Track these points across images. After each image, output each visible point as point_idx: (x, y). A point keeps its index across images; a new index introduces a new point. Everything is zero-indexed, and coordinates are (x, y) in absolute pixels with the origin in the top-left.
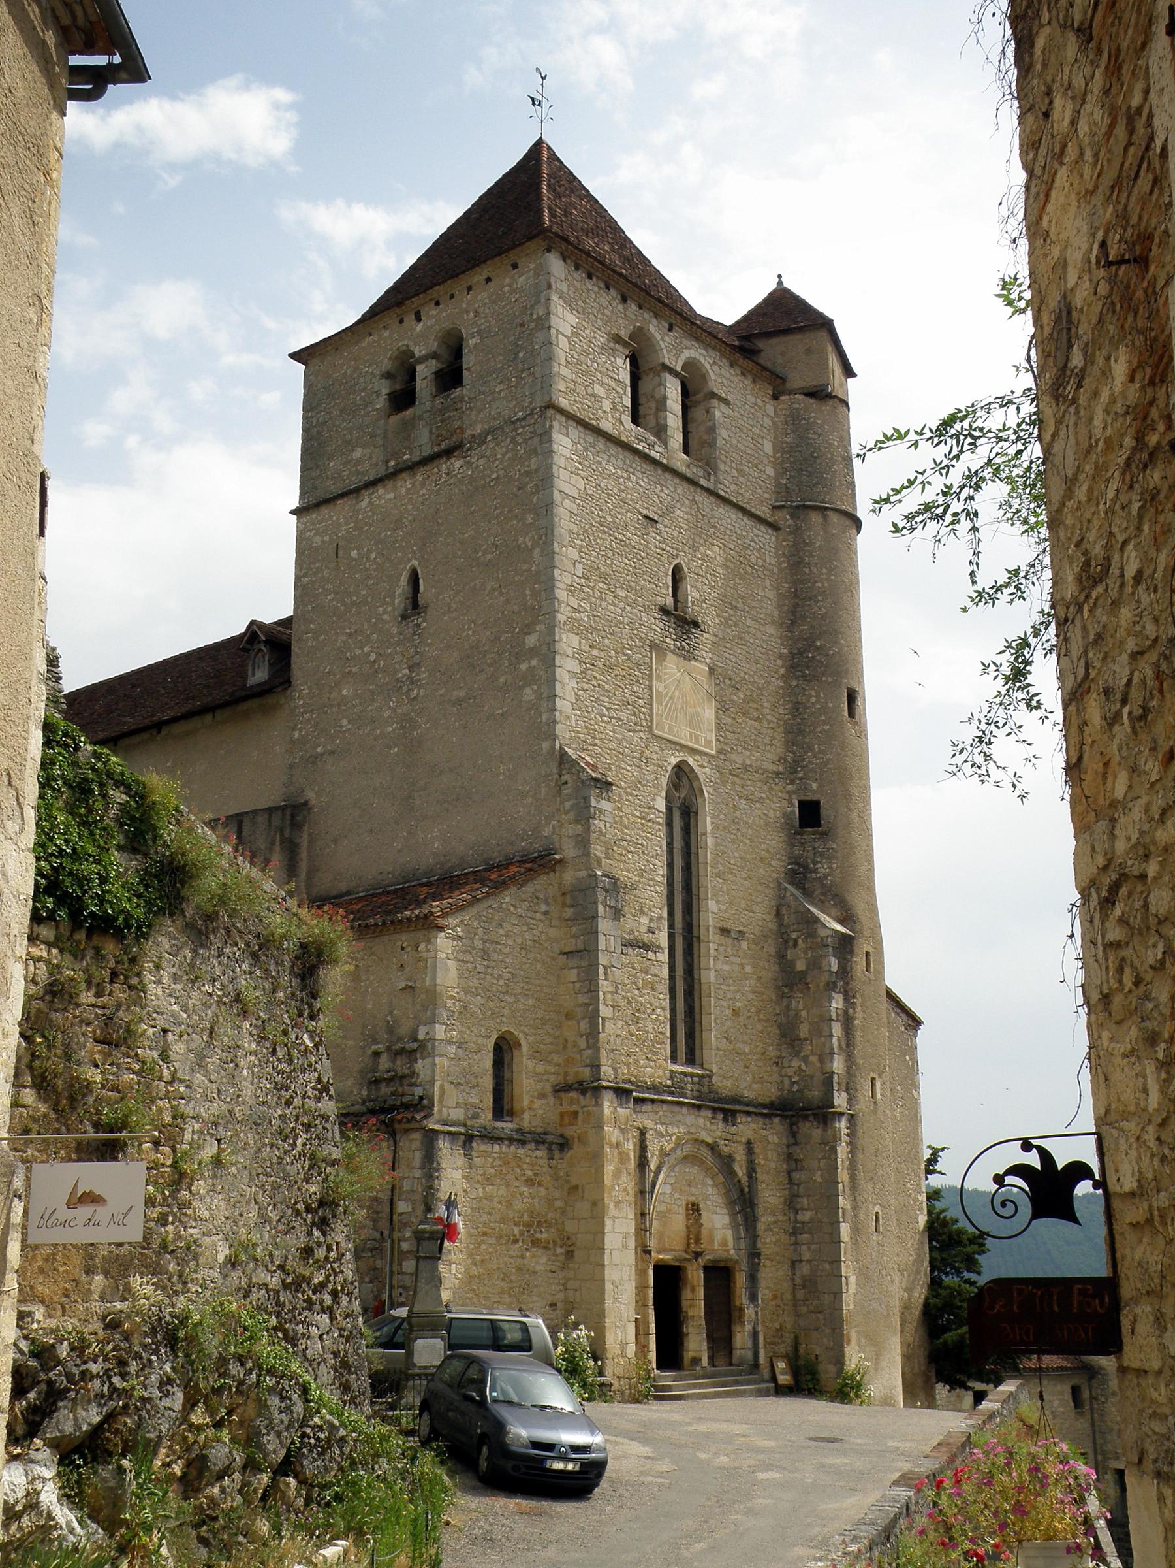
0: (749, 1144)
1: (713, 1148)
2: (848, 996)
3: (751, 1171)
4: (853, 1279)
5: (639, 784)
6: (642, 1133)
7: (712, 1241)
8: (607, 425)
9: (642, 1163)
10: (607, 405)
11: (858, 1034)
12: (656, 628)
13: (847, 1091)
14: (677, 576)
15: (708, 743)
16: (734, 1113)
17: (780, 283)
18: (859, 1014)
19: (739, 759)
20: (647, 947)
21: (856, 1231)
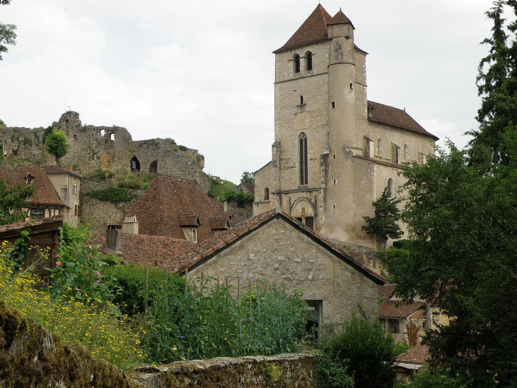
0: (316, 197)
1: (307, 198)
2: (326, 166)
3: (316, 201)
4: (323, 218)
5: (291, 140)
6: (290, 198)
7: (308, 213)
8: (286, 79)
9: (290, 203)
10: (286, 75)
11: (330, 173)
12: (296, 110)
13: (325, 183)
14: (302, 98)
15: (308, 126)
16: (312, 191)
17: (340, 10)
18: (330, 168)
19: (315, 126)
20: (293, 167)
21: (325, 209)
